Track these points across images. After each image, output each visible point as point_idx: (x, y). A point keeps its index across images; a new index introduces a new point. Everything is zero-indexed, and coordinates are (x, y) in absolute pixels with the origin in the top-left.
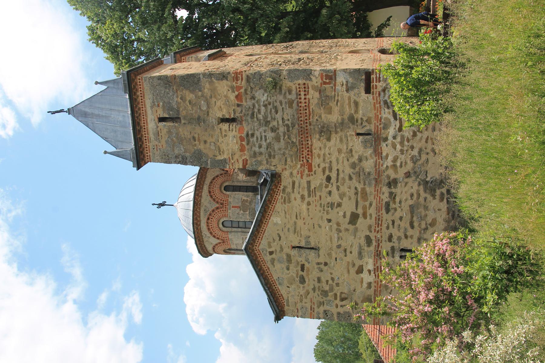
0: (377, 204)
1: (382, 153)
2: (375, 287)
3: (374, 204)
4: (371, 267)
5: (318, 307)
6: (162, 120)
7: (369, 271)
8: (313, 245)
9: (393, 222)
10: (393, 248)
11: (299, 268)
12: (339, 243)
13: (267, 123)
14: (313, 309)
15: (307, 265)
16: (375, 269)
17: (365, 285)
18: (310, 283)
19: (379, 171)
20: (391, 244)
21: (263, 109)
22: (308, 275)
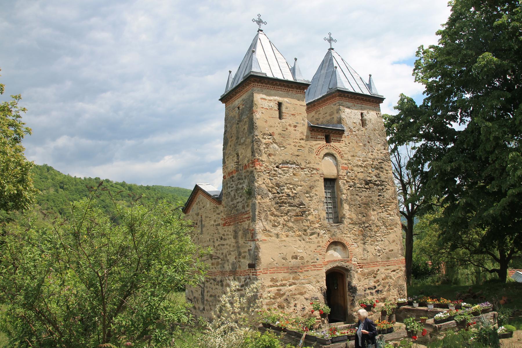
6: (239, 108)
13: (237, 190)
21: (240, 186)
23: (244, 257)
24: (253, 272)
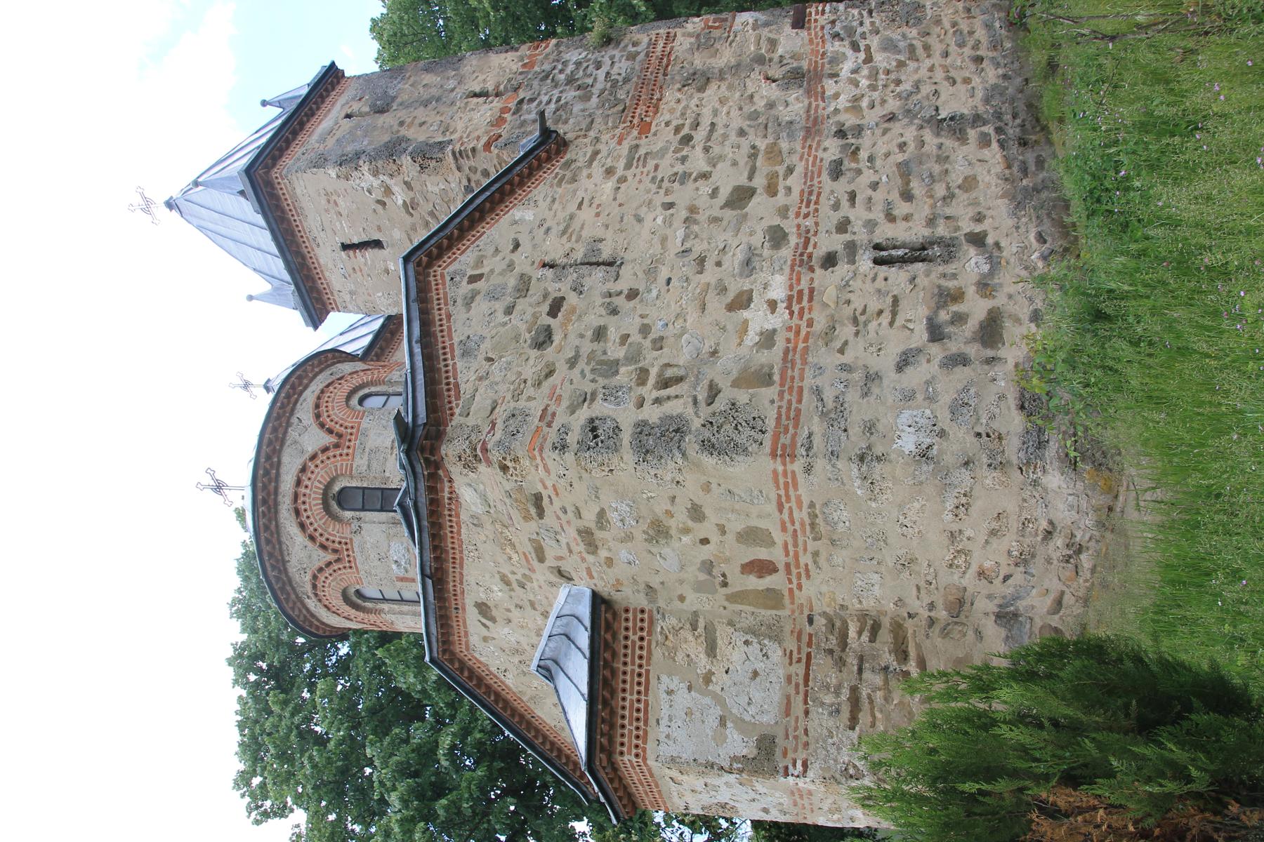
0: (807, 169)
1: (824, 93)
2: (788, 341)
3: (799, 169)
4: (778, 291)
5: (572, 410)
7: (773, 305)
8: (605, 255)
9: (852, 197)
10: (851, 248)
11: (546, 308)
12: (687, 245)
14: (549, 418)
15: (572, 299)
16: (790, 298)
17: (752, 337)
18: (569, 337)
19: (816, 119)
20: (847, 237)
22: (564, 325)
23: (773, 43)
24: (817, 13)
